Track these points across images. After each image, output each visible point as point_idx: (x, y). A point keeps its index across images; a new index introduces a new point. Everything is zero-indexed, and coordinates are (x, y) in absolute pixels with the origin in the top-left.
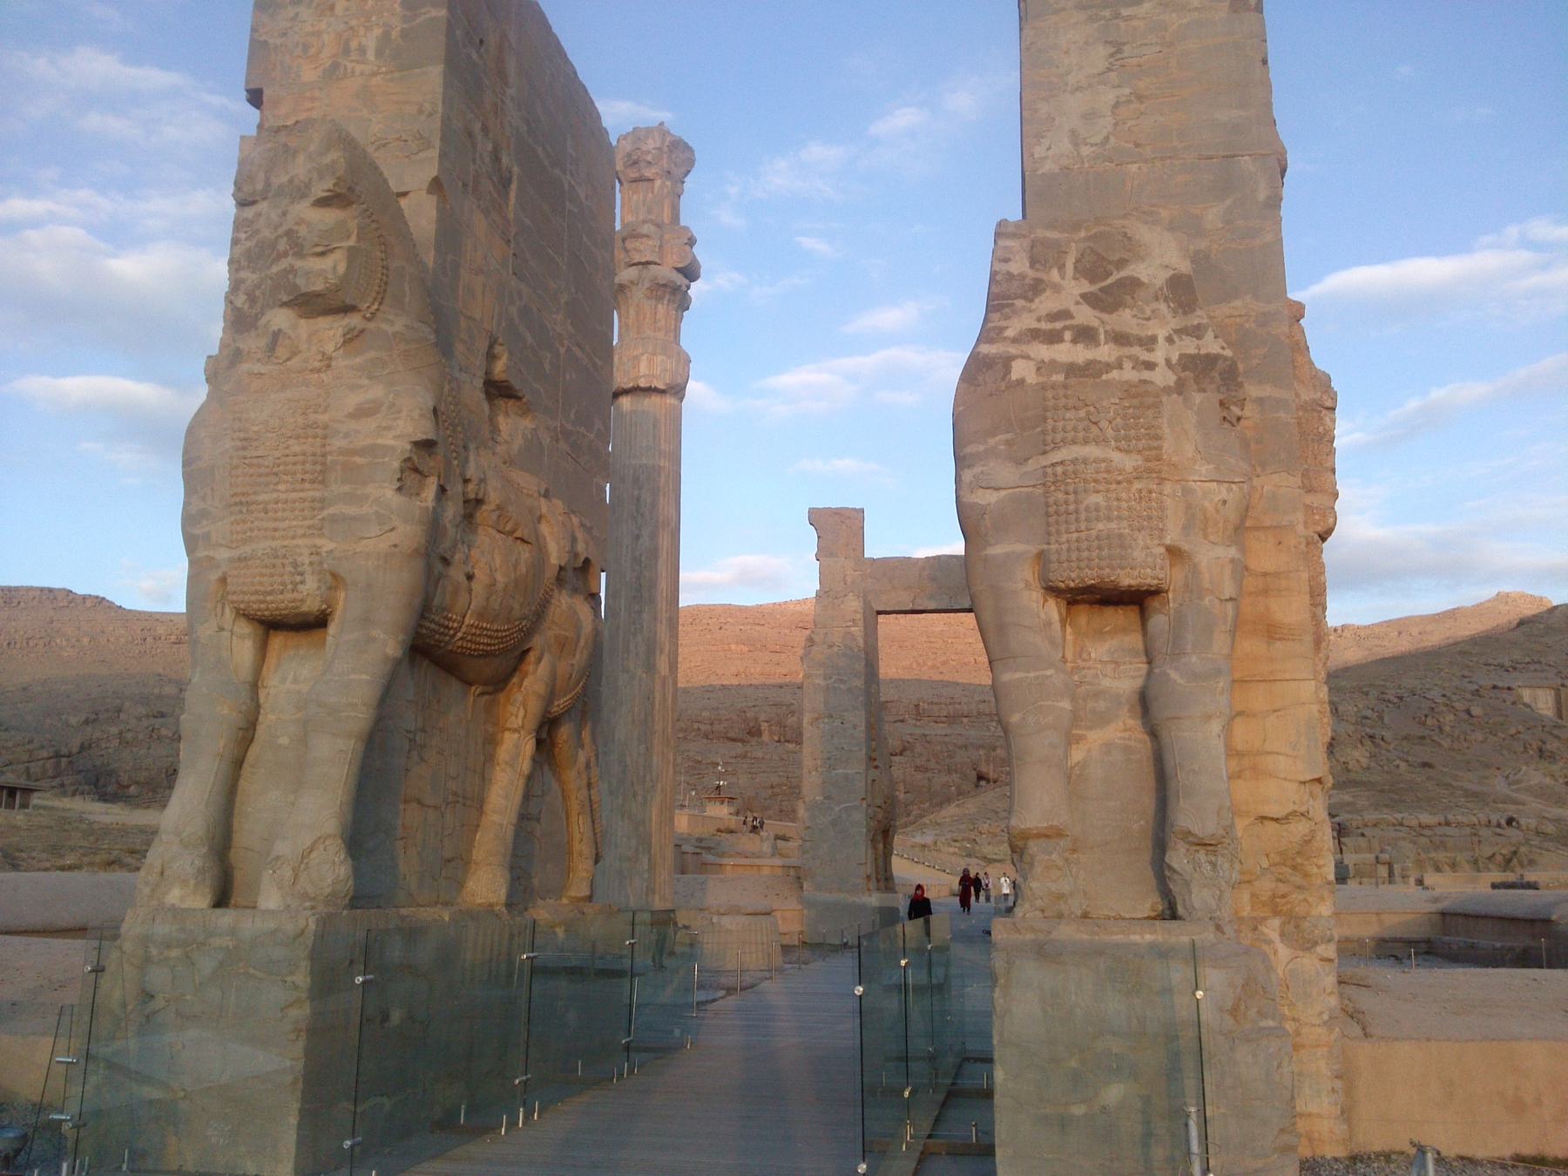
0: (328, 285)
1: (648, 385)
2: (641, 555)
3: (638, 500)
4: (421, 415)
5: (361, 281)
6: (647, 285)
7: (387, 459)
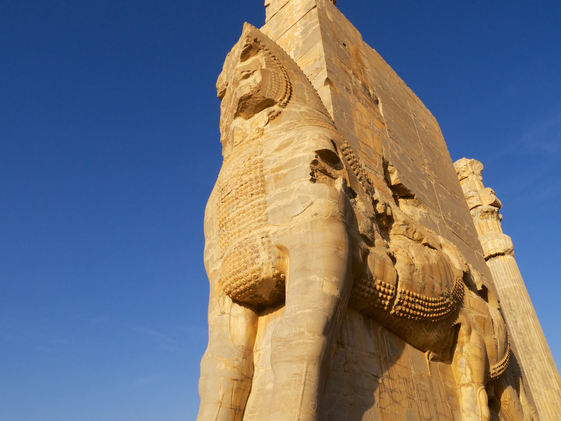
0: (252, 90)
1: (495, 253)
2: (521, 330)
3: (509, 304)
4: (320, 137)
5: (274, 87)
6: (479, 214)
7: (301, 165)
